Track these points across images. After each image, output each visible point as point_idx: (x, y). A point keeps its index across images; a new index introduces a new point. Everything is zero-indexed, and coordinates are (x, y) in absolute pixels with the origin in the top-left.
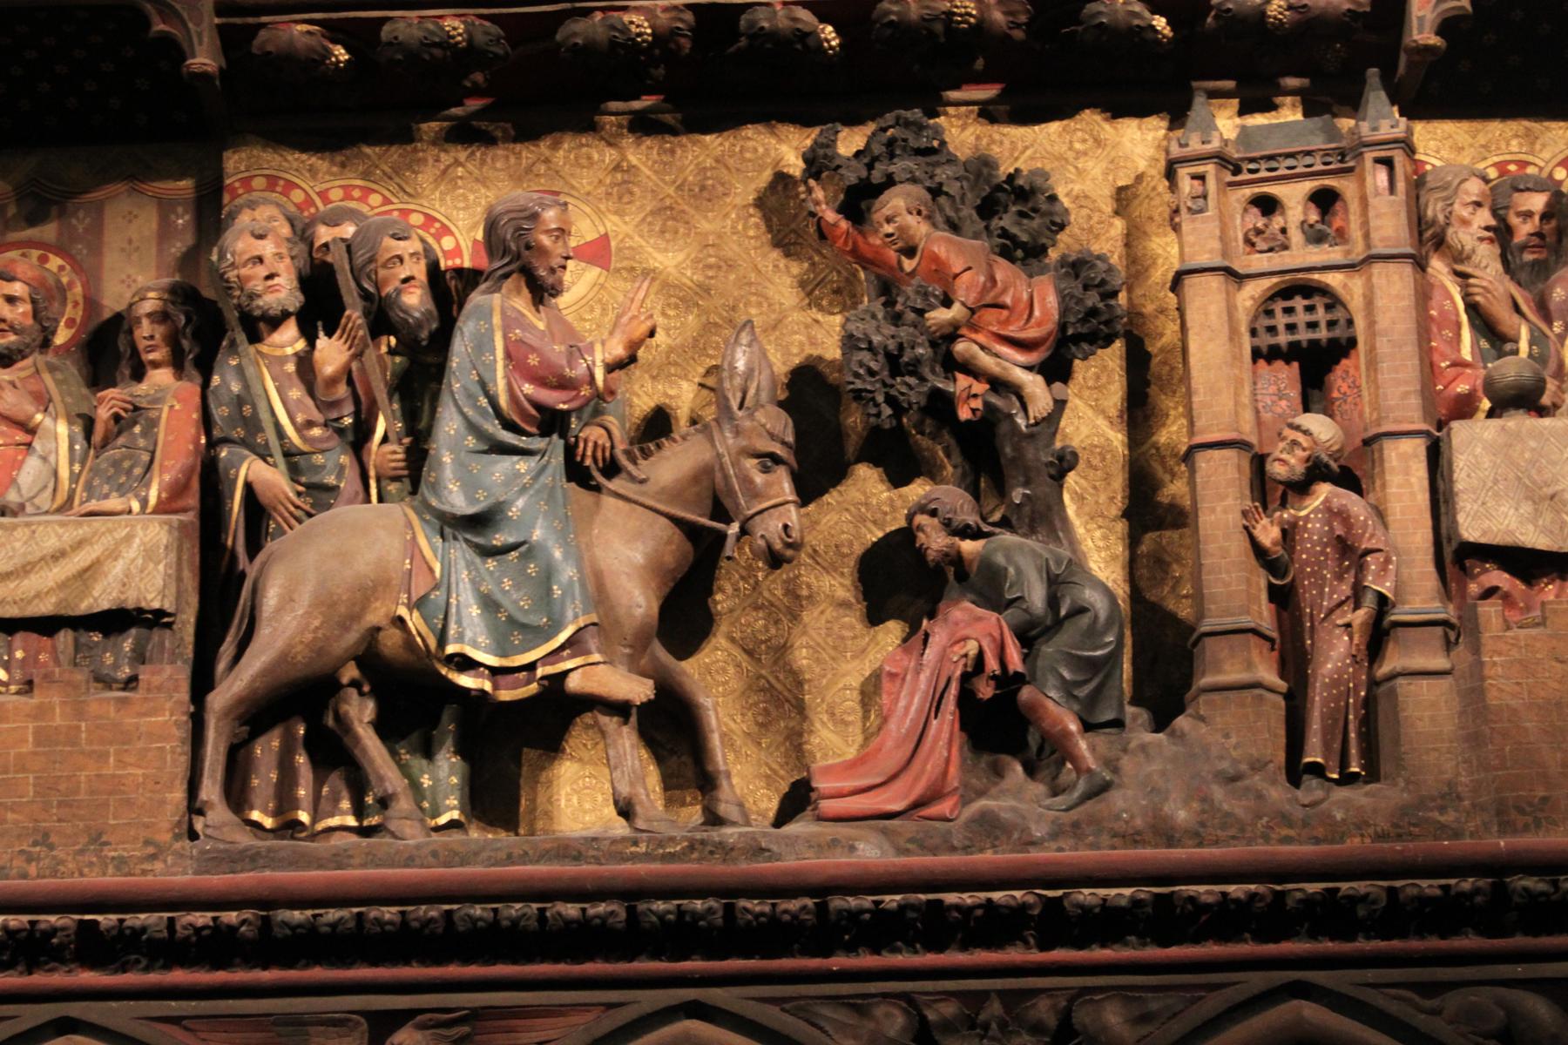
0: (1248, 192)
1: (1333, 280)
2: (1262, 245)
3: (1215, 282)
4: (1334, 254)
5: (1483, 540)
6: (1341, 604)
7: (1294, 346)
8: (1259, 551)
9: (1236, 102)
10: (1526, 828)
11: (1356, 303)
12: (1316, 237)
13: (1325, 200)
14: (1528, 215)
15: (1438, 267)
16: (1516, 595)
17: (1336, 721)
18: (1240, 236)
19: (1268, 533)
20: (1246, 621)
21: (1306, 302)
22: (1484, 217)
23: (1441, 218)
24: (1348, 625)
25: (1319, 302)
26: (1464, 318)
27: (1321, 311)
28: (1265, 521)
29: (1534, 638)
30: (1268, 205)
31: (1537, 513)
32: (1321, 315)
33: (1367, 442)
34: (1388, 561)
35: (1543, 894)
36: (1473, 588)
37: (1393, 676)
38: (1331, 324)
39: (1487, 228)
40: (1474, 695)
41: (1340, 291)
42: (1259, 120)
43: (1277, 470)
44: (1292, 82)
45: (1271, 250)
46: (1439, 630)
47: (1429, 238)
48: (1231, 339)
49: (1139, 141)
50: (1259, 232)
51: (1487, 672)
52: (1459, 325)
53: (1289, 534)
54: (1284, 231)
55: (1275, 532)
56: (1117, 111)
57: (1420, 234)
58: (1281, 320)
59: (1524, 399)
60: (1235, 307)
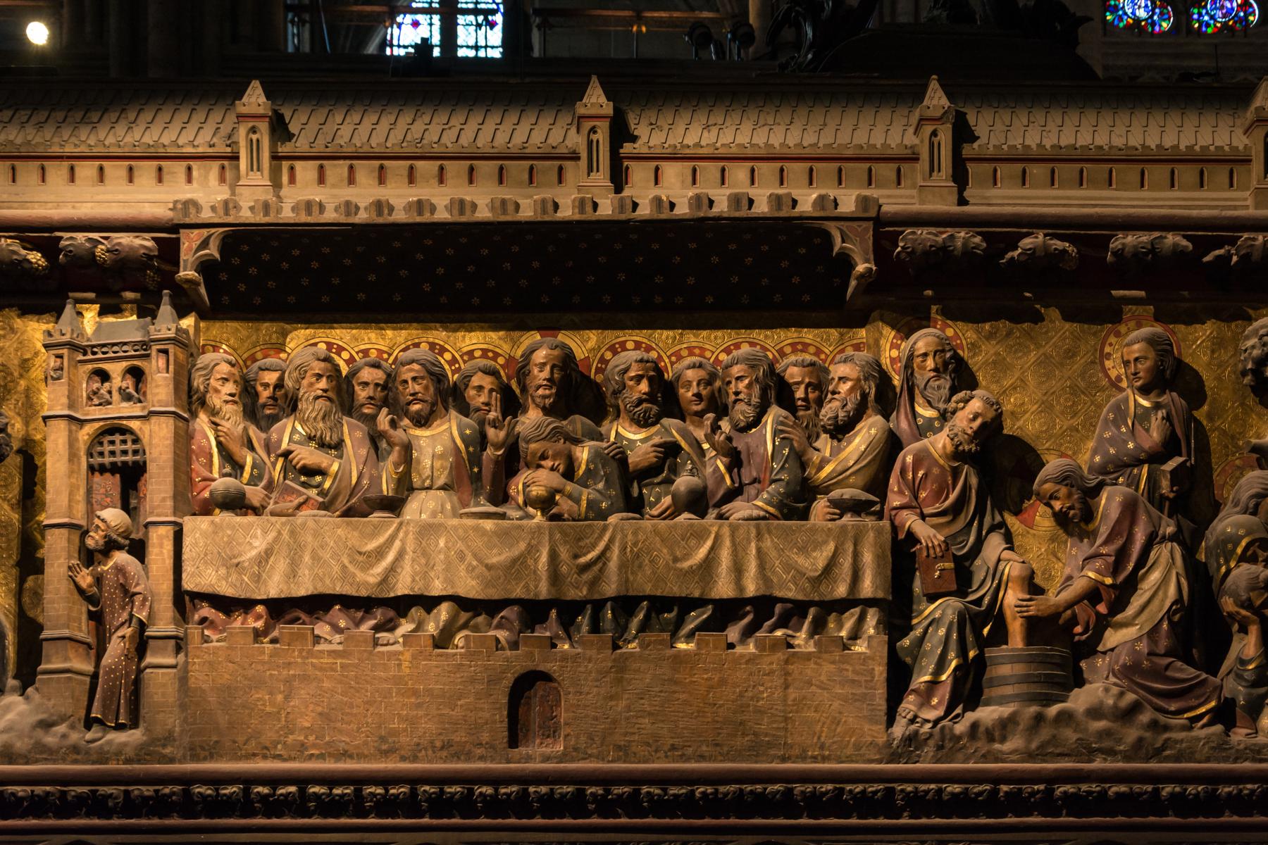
0: (90, 367)
1: (134, 425)
2: (96, 401)
3: (62, 424)
4: (137, 410)
5: (195, 590)
6: (123, 624)
7: (114, 464)
8: (81, 591)
9: (98, 306)
10: (205, 759)
11: (145, 440)
12: (127, 398)
13: (137, 374)
14: (266, 385)
15: (203, 420)
16: (218, 621)
17: (113, 693)
18: (85, 394)
19: (85, 579)
20: (66, 632)
21: (122, 437)
22: (230, 388)
23: (202, 388)
24: (123, 637)
25: (129, 437)
26: (215, 450)
27: (129, 443)
28: (85, 571)
29: (218, 648)
30: (104, 376)
31: (229, 574)
32: (129, 446)
33: (146, 526)
34: (145, 600)
35: (209, 796)
36: (196, 617)
37: (146, 668)
38: (135, 452)
39: (231, 395)
40: (183, 680)
41: (138, 432)
42: (110, 319)
43: (90, 543)
44: (129, 295)
45: (100, 404)
46: (173, 642)
47: (192, 399)
48: (70, 460)
49: (35, 330)
50: (95, 393)
51: (190, 668)
52: (211, 456)
53: (99, 580)
54: (110, 392)
55: (89, 579)
56: (25, 311)
57: (190, 397)
58: (107, 448)
59: (236, 503)
60: (77, 440)
